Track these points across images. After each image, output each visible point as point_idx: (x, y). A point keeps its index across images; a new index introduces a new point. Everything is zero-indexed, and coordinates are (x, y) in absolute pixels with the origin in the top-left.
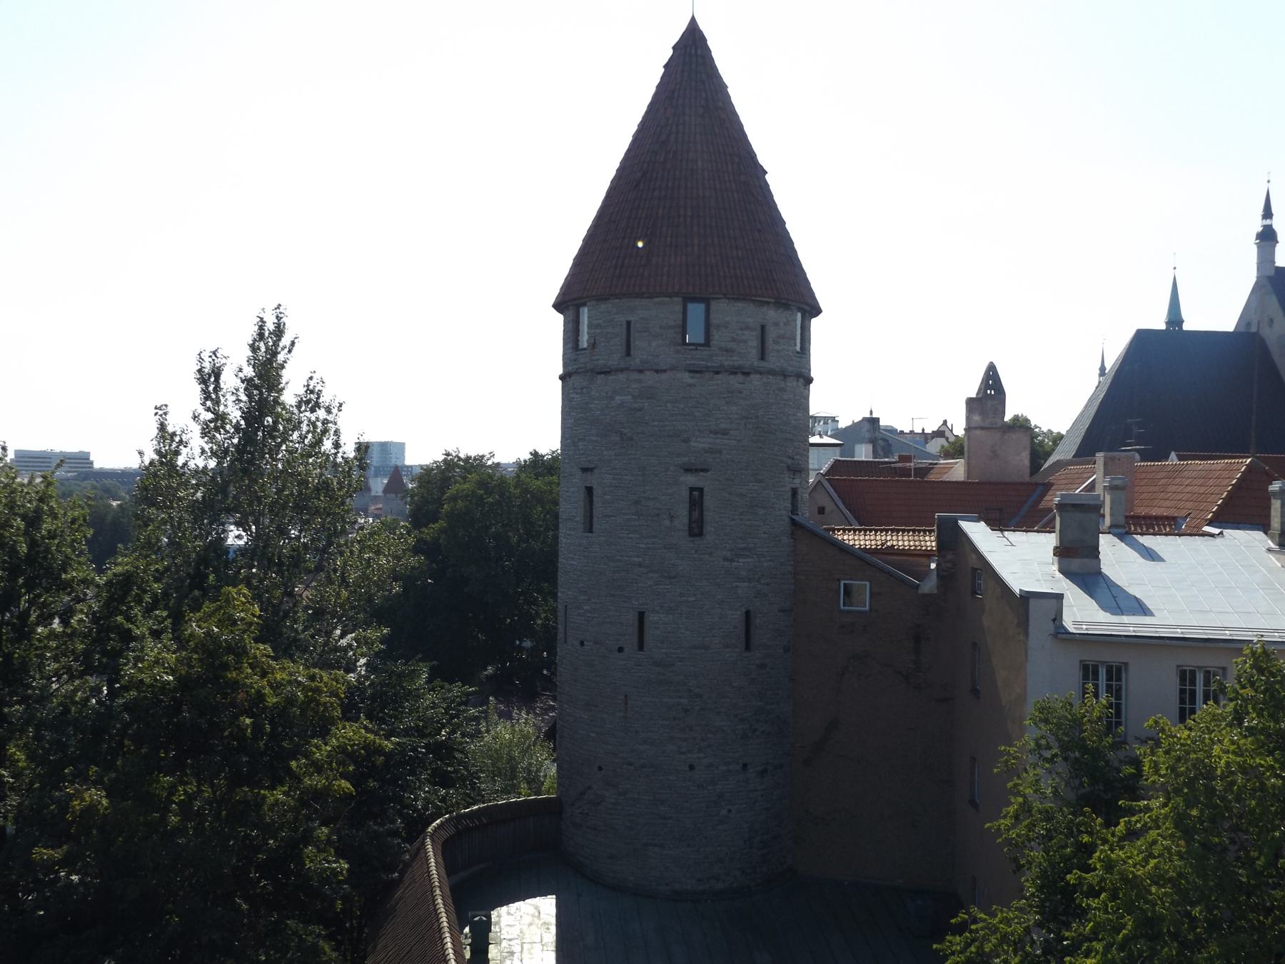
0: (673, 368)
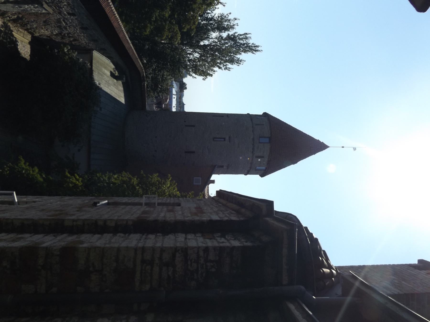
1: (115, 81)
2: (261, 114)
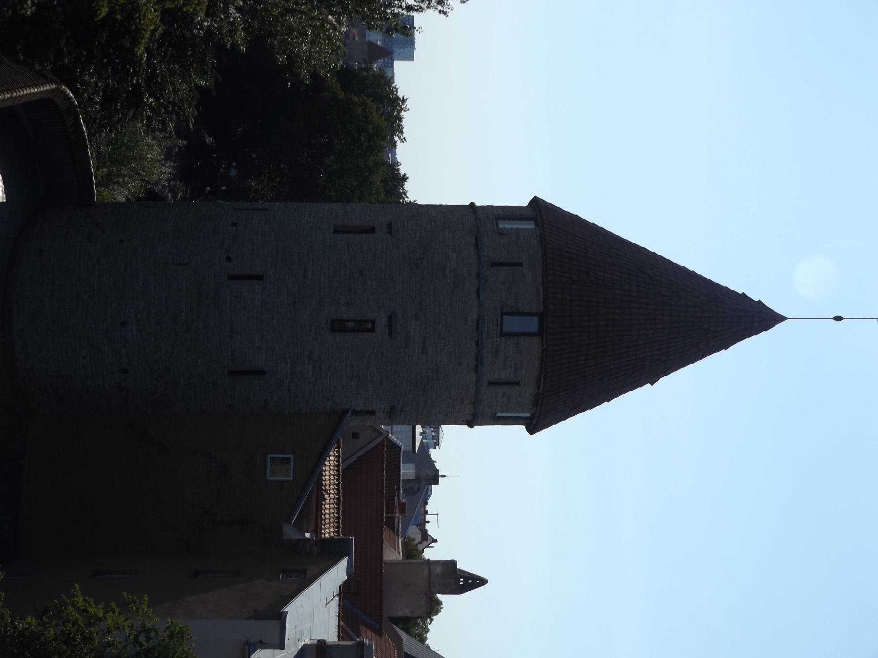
2: (523, 201)
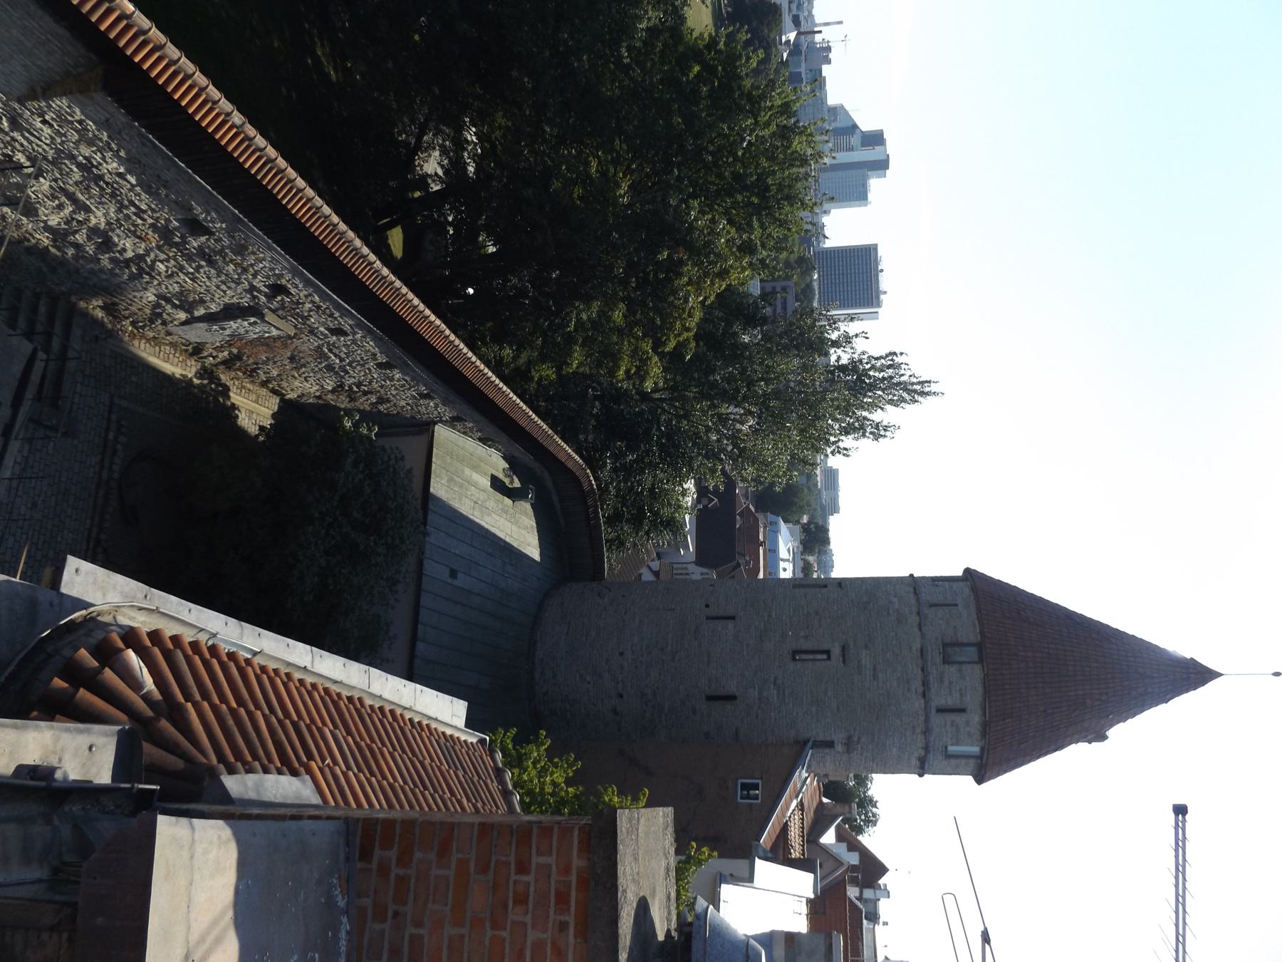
0: (923, 636)
1: (508, 501)
